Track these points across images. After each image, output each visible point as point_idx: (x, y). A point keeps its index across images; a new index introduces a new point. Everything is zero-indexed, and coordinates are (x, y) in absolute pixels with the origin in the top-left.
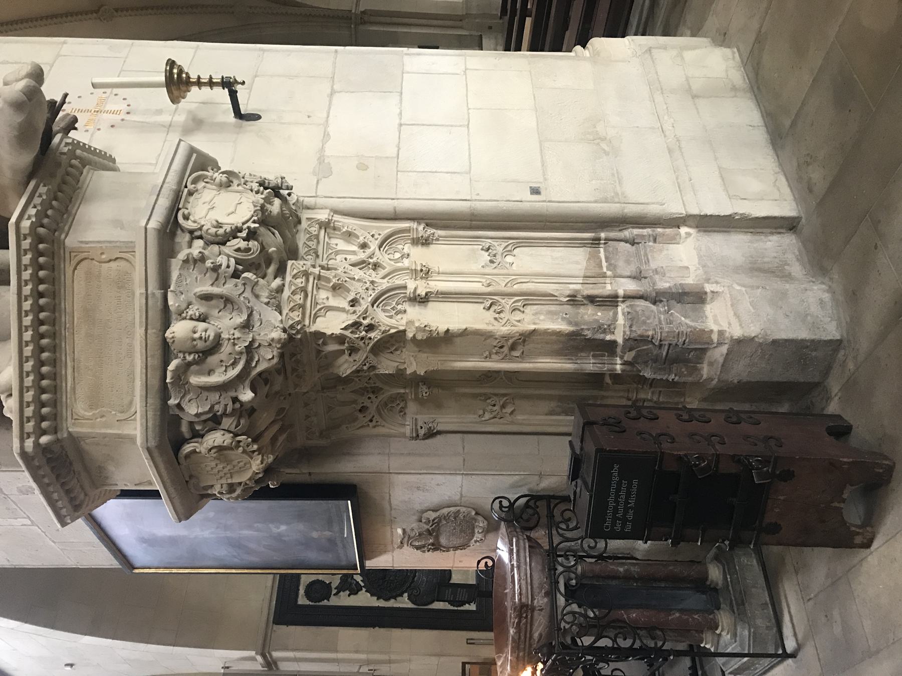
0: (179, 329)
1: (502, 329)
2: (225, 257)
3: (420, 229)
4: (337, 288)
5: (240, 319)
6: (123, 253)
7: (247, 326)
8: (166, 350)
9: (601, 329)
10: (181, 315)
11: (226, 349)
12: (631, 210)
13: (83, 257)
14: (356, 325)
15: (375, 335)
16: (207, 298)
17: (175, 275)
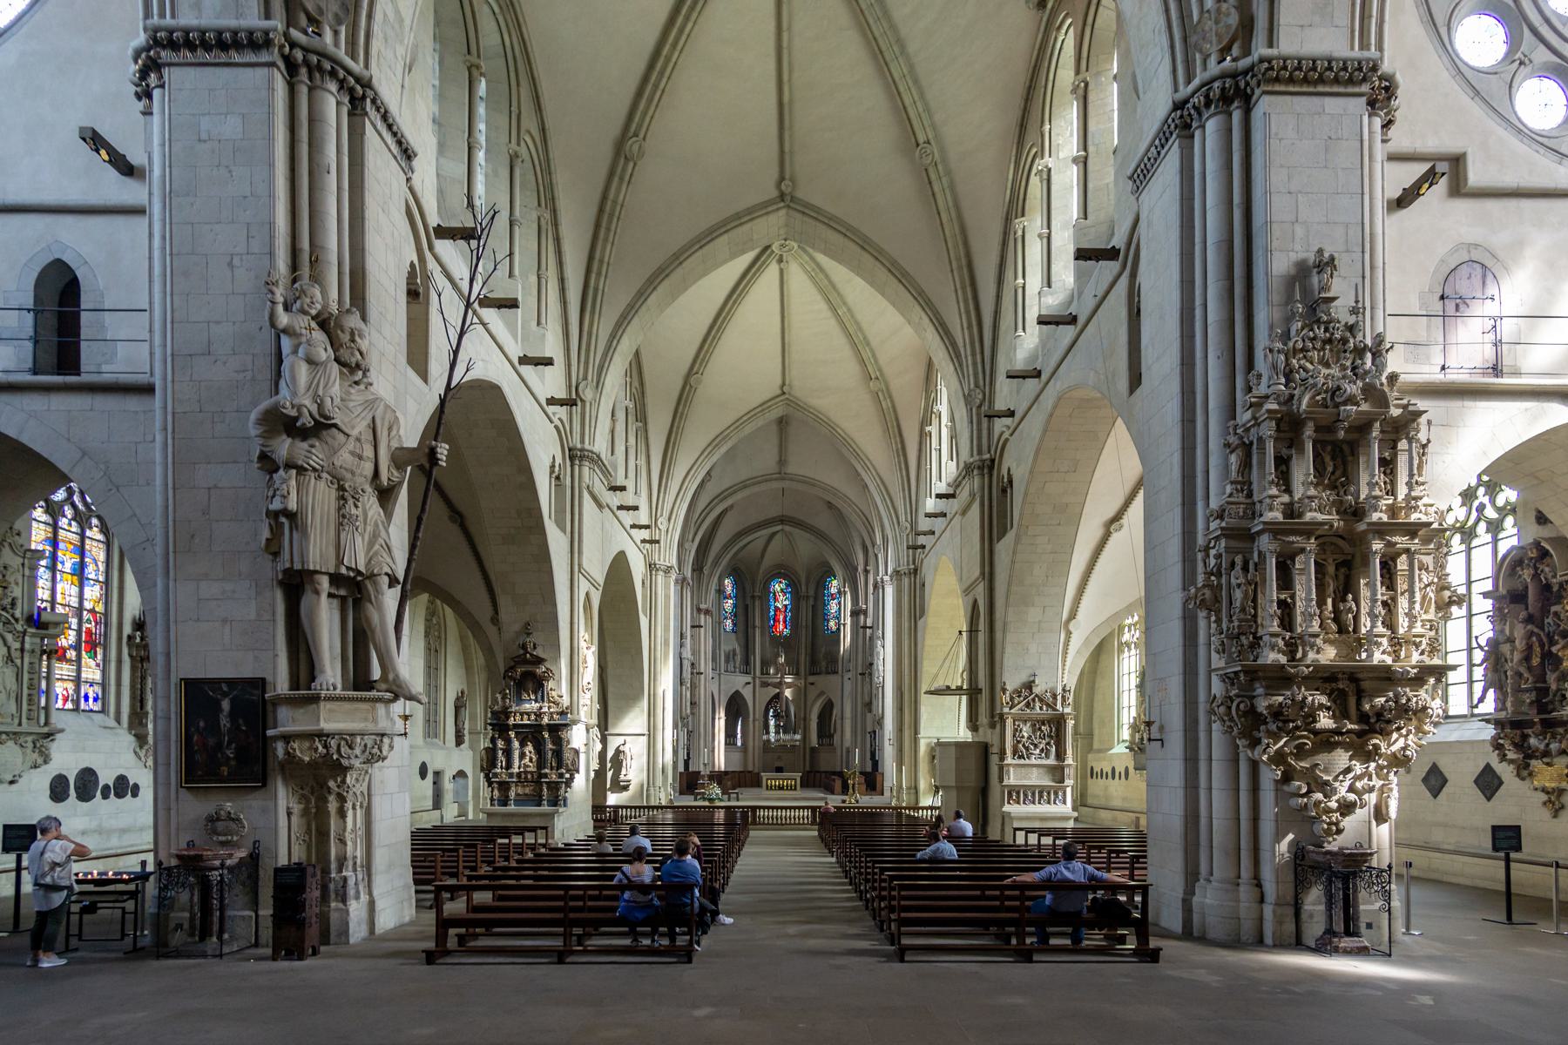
0: (358, 739)
1: (347, 834)
2: (375, 750)
3: (365, 805)
4: (357, 780)
5: (358, 754)
6: (375, 721)
7: (356, 757)
8: (352, 735)
9: (347, 867)
10: (362, 739)
11: (350, 751)
12: (373, 877)
13: (374, 709)
14: (349, 787)
15: (345, 794)
16: (365, 746)
17: (373, 737)
